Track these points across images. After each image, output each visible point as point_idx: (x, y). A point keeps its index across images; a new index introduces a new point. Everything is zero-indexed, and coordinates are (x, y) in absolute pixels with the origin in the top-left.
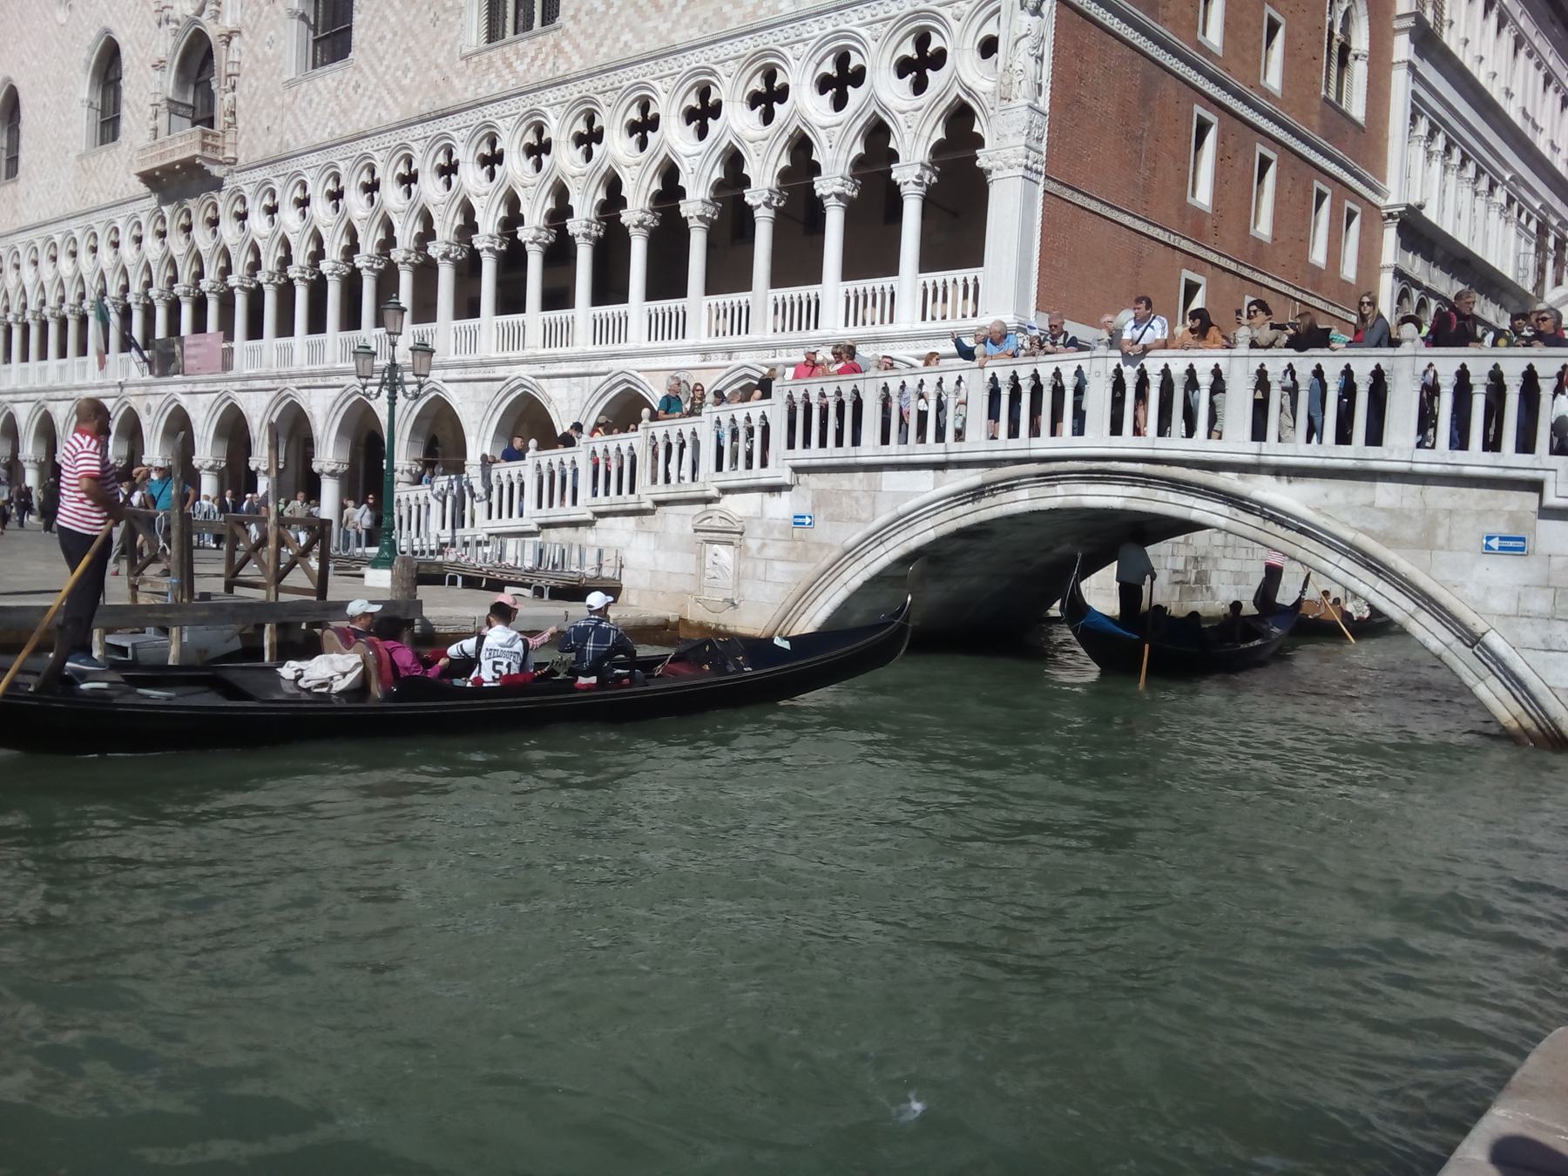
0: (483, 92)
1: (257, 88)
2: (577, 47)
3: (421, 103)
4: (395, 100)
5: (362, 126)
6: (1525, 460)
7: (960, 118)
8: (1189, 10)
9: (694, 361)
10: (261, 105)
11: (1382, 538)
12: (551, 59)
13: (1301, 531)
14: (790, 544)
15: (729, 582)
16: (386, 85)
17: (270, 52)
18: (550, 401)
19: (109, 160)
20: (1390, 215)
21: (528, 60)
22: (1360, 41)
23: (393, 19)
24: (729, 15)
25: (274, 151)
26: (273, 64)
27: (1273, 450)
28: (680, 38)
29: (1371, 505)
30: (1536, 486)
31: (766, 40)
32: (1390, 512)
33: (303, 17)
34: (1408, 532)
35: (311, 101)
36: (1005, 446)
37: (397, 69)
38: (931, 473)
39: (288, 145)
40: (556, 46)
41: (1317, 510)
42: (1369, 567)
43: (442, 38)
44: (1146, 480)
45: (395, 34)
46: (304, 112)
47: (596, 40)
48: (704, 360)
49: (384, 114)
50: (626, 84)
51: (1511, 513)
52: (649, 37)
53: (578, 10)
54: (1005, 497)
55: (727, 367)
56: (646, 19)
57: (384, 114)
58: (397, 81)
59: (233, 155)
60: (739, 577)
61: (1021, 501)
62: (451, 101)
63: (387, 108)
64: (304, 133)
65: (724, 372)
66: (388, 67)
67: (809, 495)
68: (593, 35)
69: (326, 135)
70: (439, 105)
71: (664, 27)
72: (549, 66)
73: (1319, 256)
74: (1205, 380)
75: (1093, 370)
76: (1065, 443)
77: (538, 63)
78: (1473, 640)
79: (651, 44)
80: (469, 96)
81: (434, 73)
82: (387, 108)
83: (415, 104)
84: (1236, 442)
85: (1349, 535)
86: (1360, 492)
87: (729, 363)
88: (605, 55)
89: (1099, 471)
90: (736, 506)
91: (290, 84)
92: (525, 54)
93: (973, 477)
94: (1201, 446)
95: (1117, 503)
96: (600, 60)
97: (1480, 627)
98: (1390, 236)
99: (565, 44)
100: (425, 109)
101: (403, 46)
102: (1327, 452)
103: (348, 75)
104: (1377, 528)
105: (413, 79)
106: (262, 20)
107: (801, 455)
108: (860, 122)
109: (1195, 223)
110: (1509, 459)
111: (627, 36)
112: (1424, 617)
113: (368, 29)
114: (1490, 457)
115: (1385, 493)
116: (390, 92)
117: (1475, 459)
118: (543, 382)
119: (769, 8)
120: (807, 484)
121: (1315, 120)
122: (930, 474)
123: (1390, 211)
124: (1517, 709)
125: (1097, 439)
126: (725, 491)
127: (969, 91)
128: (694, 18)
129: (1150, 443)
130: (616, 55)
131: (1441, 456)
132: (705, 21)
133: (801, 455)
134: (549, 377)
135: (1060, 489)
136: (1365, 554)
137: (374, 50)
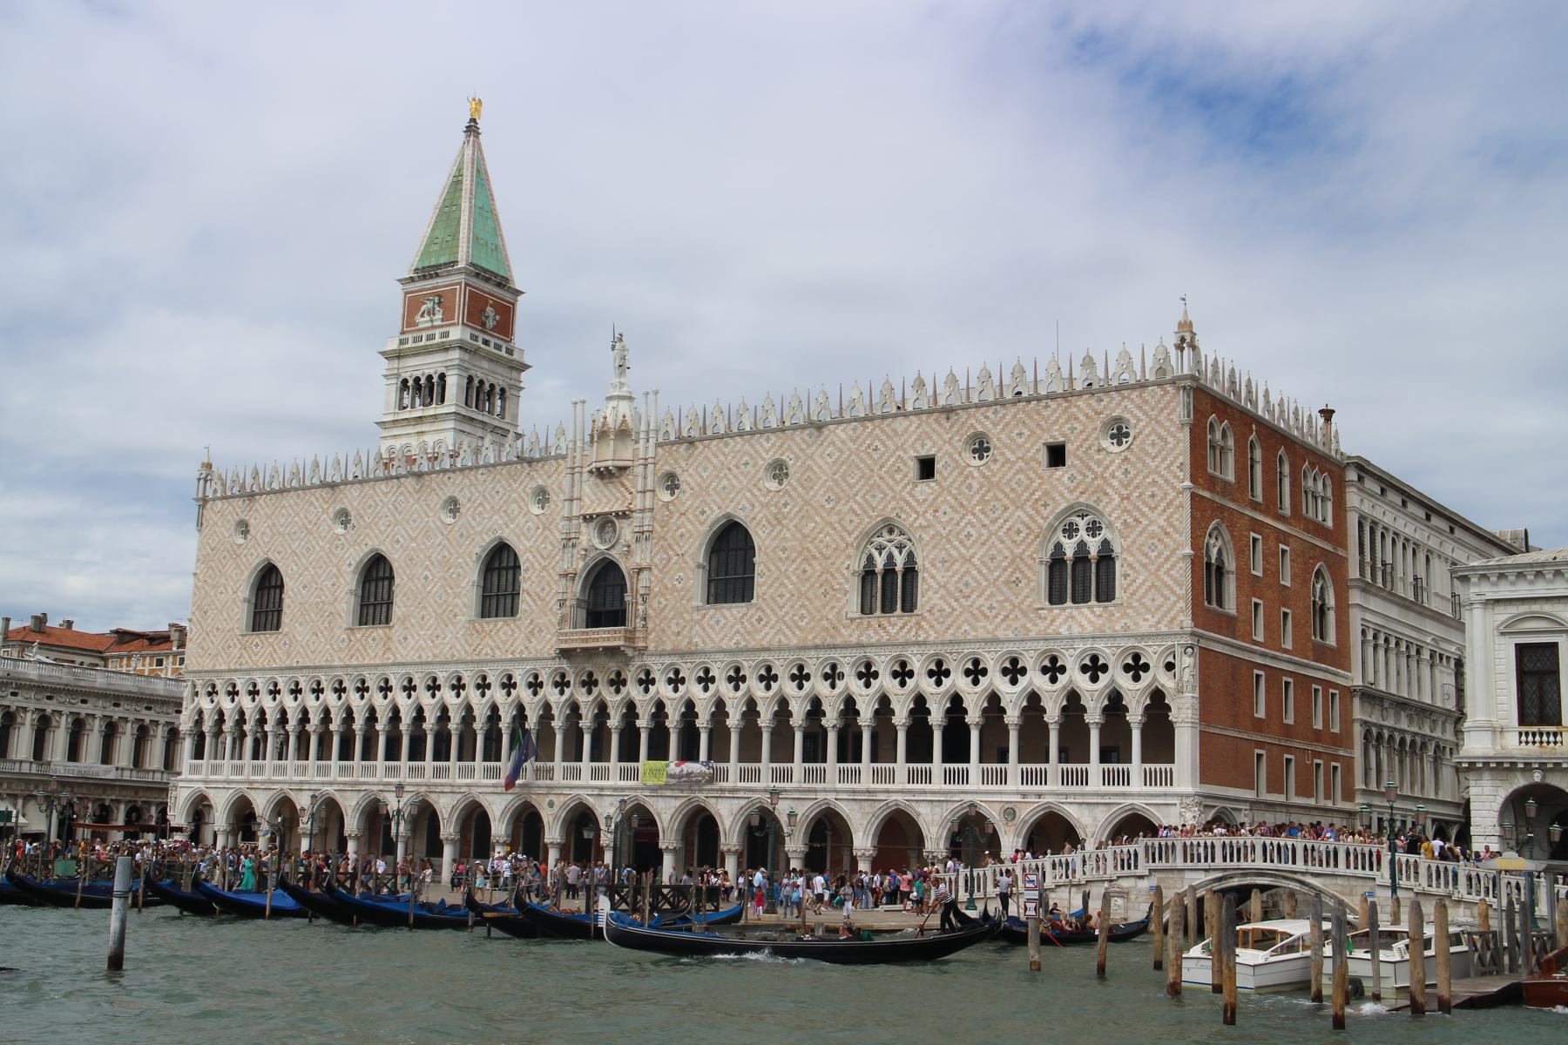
0: (864, 639)
1: (666, 606)
2: (932, 626)
3: (814, 638)
4: (794, 633)
5: (765, 643)
6: (1371, 873)
7: (1157, 696)
8: (1249, 628)
9: (1018, 799)
10: (670, 616)
12: (914, 630)
15: (1122, 911)
16: (785, 624)
17: (679, 586)
18: (919, 815)
19: (506, 628)
21: (897, 628)
22: (1331, 601)
23: (790, 587)
25: (683, 645)
26: (682, 593)
27: (1311, 868)
28: (1000, 634)
30: (1374, 879)
31: (1051, 645)
33: (704, 567)
34: (1347, 891)
35: (718, 622)
36: (1228, 864)
37: (795, 615)
39: (696, 645)
40: (918, 623)
43: (831, 605)
45: (793, 595)
46: (712, 627)
47: (946, 625)
49: (783, 639)
50: (966, 651)
52: (980, 630)
53: (932, 608)
54: (1230, 880)
56: (978, 620)
57: (783, 639)
58: (796, 623)
59: (644, 644)
60: (1127, 909)
62: (839, 640)
63: (785, 636)
64: (712, 639)
66: (787, 613)
68: (943, 622)
69: (732, 644)
70: (829, 641)
71: (991, 627)
72: (913, 633)
73: (1319, 726)
74: (1290, 847)
76: (1249, 865)
77: (905, 630)
79: (982, 634)
80: (854, 640)
81: (825, 623)
82: (785, 636)
83: (810, 638)
84: (1300, 866)
86: (1334, 881)
88: (952, 634)
89: (1260, 873)
90: (1125, 883)
91: (698, 609)
92: (895, 625)
93: (1220, 874)
94: (1290, 866)
95: (1266, 883)
96: (948, 637)
98: (1356, 701)
99: (923, 623)
100: (818, 641)
101: (799, 603)
102: (1324, 870)
103: (751, 612)
105: (807, 623)
106: (671, 564)
107: (1152, 865)
108: (1107, 691)
109: (1258, 726)
110: (1367, 872)
111: (966, 627)
113: (770, 587)
115: (1340, 881)
116: (788, 627)
118: (913, 804)
121: (1310, 654)
125: (1259, 864)
127: (1163, 686)
128: (1009, 626)
129: (1276, 865)
130: (961, 638)
131: (1351, 871)
132: (1016, 629)
133: (1152, 865)
134: (916, 801)
137: (776, 602)
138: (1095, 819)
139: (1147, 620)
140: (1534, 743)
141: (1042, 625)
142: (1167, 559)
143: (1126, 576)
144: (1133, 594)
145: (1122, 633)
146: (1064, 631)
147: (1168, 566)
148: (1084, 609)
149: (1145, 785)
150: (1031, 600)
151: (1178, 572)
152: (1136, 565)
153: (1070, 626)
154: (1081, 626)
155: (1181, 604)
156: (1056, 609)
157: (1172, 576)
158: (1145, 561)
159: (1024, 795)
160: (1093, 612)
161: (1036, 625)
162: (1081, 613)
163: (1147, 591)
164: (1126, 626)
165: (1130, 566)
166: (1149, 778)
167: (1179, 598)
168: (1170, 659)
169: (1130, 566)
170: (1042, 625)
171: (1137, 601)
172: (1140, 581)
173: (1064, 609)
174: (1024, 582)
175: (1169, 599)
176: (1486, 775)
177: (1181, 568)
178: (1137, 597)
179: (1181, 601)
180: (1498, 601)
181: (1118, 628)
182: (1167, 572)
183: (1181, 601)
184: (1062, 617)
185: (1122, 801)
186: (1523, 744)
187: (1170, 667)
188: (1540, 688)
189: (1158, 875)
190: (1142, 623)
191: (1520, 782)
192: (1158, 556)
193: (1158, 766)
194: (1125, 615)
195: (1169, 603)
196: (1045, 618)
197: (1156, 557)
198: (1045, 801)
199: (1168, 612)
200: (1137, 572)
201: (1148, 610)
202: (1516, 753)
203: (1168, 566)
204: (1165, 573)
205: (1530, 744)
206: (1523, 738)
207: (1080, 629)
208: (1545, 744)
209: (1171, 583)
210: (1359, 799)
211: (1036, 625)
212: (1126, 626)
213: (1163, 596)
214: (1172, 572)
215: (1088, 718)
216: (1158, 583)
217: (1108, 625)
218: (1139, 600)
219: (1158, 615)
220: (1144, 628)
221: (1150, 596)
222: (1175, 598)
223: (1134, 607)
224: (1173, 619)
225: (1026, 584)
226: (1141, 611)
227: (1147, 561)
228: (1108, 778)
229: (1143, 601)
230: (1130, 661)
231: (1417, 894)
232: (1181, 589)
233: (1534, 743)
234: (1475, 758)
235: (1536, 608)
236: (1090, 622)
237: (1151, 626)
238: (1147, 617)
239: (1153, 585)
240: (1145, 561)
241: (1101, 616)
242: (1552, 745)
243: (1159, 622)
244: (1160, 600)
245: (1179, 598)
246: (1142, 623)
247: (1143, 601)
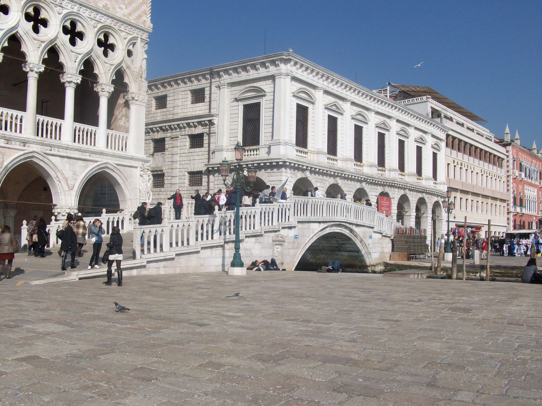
48: (7, 143)
54: (326, 229)
55: (22, 150)
65: (22, 153)
87: (23, 148)
95: (338, 231)
122: (317, 224)
138: (74, 174)
145: (104, 11)
149: (107, 147)
185: (100, 160)
198: (31, 150)
215: (65, 79)
219: (130, 9)
220: (119, 14)
237: (124, 15)
243: (130, 14)
246: (118, 10)
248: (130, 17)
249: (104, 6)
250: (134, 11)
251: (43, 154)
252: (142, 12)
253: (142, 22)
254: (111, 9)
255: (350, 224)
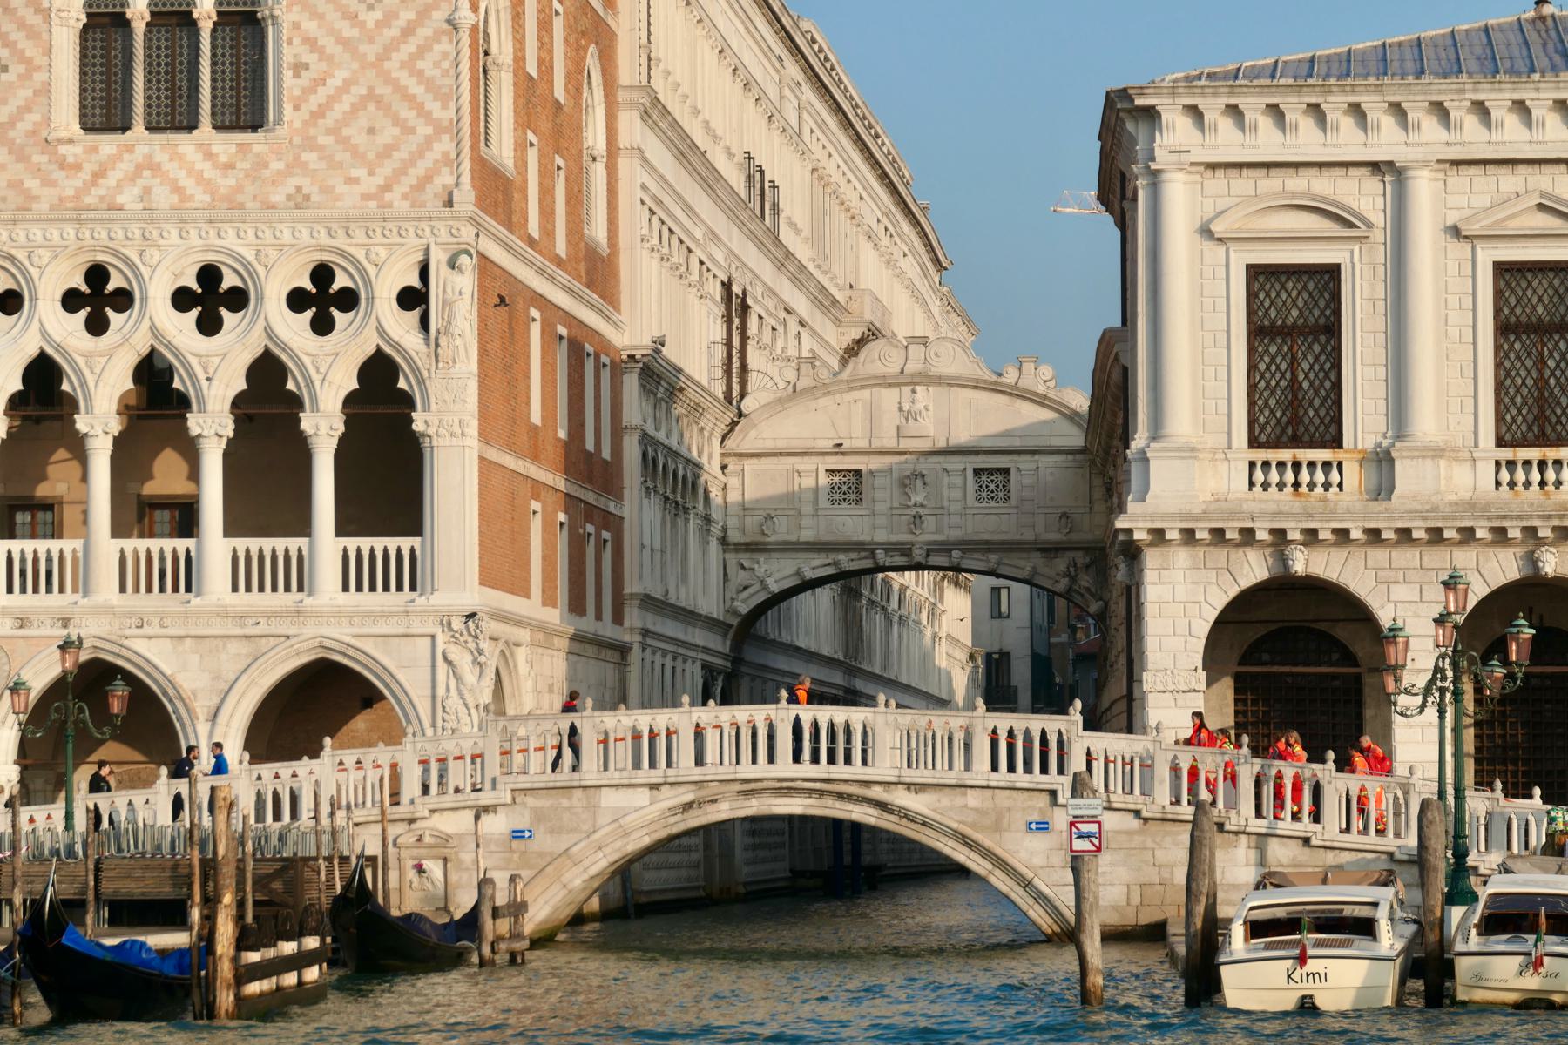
6: (1044, 778)
11: (973, 826)
13: (924, 824)
14: (507, 855)
20: (631, 357)
24: (35, 192)
29: (966, 806)
30: (1053, 793)
32: (976, 810)
38: (646, 790)
41: (935, 811)
42: (966, 844)
44: (822, 793)
48: (21, 627)
51: (1040, 809)
54: (710, 808)
61: (723, 811)
67: (527, 813)
75: (779, 717)
76: (762, 769)
78: (1027, 885)
85: (955, 825)
89: (786, 788)
97: (1030, 875)
98: (631, 383)
104: (969, 820)
112: (998, 872)
114: (1028, 776)
117: (1020, 778)
119: (102, 198)
120: (524, 804)
123: (633, 353)
124: (1050, 921)
125: (785, 767)
126: (433, 811)
135: (754, 802)
136: (964, 836)
139: (352, 181)
140: (1281, 486)
141: (70, 185)
142: (408, 31)
143: (299, 68)
144: (319, 114)
146: (127, 198)
147: (410, 47)
148: (185, 143)
150: (35, 117)
151: (437, 65)
152: (327, 43)
153: (147, 191)
154: (178, 190)
155: (446, 144)
156: (108, 144)
157: (420, 73)
158: (349, 31)
159: (22, 622)
160: (209, 156)
161: (51, 183)
162: (176, 157)
163: (355, 109)
164: (300, 200)
165: (311, 43)
166: (357, 575)
167: (439, 130)
168: (415, 282)
169: (311, 43)
170: (70, 185)
171: (329, 132)
172: (336, 80)
173: (130, 148)
174: (16, 70)
175: (412, 131)
176: (1183, 556)
177: (445, 55)
178: (329, 120)
179: (446, 138)
180: (1213, 166)
181: (278, 197)
182: (409, 65)
183: (446, 138)
184: (125, 166)
186: (1258, 489)
187: (412, 299)
188: (1293, 364)
189: (531, 801)
190: (341, 188)
191: (1254, 569)
192: (390, 17)
193: (379, 543)
194: (296, 165)
195: (412, 143)
196: (77, 167)
197: (379, 24)
199: (412, 162)
200: (330, 59)
201: (358, 155)
202: (1249, 506)
203: (410, 47)
204: (403, 65)
205: (1273, 489)
206: (1259, 476)
207: (175, 199)
208: (1304, 489)
209: (418, 90)
210: (634, 617)
211: (51, 183)
212: (300, 200)
213: (396, 121)
214: (420, 65)
216: (383, 90)
217: (250, 189)
218: (334, 131)
219: (386, 169)
220: (349, 199)
221: (363, 121)
222: (429, 130)
223: (321, 148)
224: (428, 178)
225: (20, 76)
226: (338, 157)
227: (355, 32)
228: (246, 575)
229: (346, 132)
230: (340, 282)
231: (1146, 820)
232: (445, 107)
233: (1281, 486)
234: (1163, 518)
235: (1298, 183)
236: (200, 180)
237: (366, 197)
238: (355, 173)
239: (371, 96)
240: (349, 31)
241: (229, 166)
242: (1319, 490)
243: (386, 188)
244: (389, 133)
245: (439, 130)
246: (341, 188)
247: (346, 132)
248: (388, 197)
249: (289, 197)
250: (402, 172)
251: (114, 638)
252: (436, 161)
253: (435, 195)
254: (315, 198)
255: (867, 783)
